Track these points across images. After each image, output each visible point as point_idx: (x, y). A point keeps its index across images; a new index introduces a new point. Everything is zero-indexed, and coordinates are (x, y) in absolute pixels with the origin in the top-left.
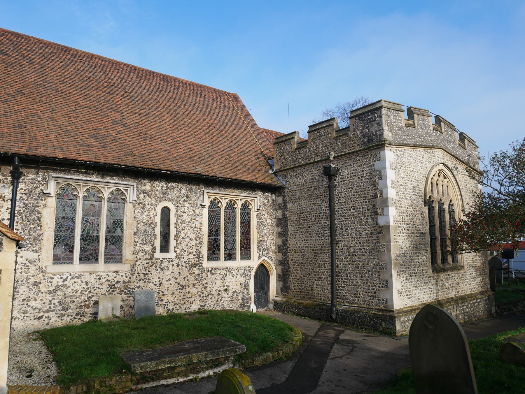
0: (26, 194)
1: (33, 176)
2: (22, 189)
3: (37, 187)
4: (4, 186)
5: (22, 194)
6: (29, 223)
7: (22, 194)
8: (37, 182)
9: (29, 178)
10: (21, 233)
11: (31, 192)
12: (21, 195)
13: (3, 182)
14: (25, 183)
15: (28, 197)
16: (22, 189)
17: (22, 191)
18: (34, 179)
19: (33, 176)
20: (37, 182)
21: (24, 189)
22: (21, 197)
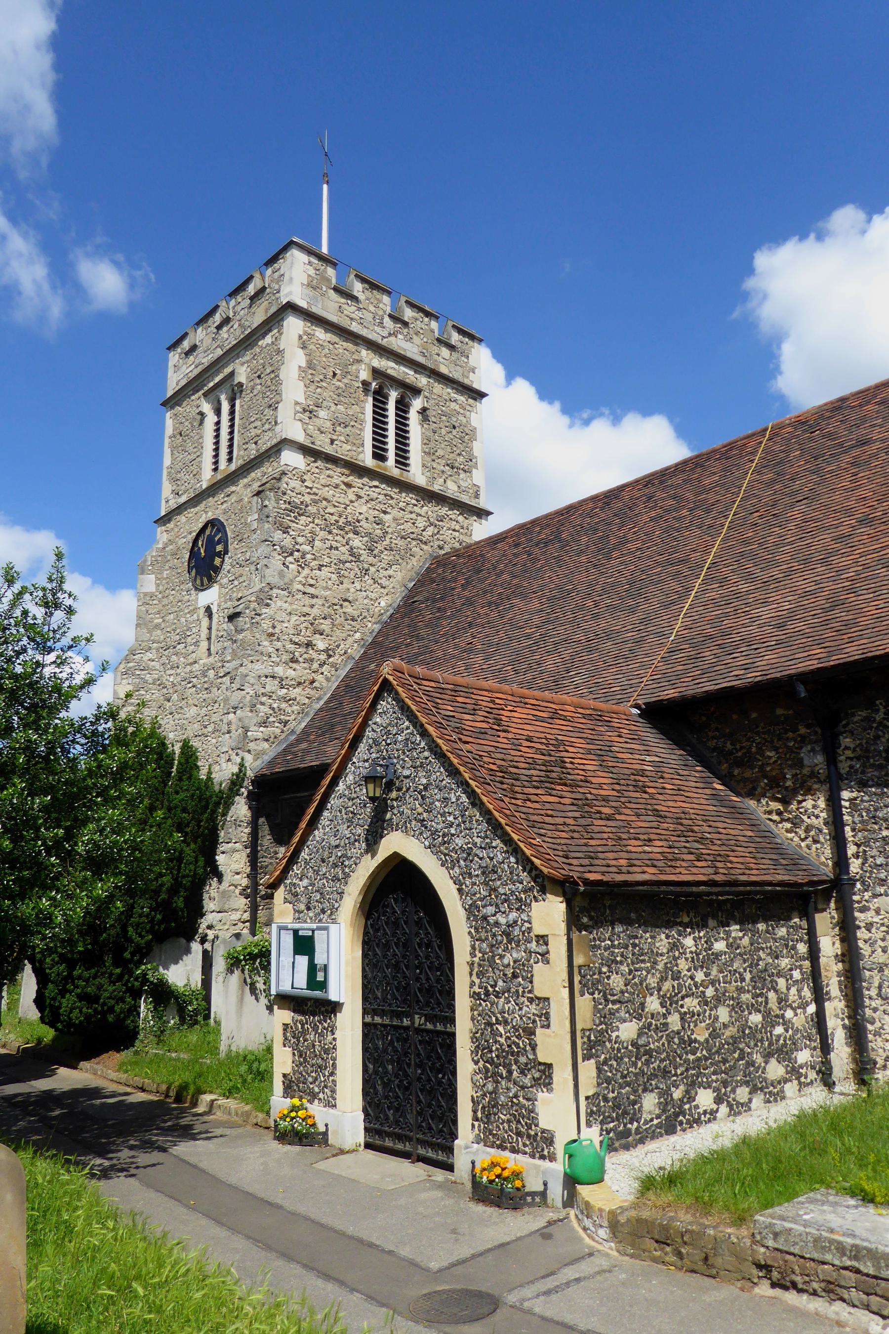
0: (858, 758)
1: (864, 714)
2: (847, 748)
3: (877, 737)
4: (813, 750)
5: (851, 759)
6: (876, 827)
7: (851, 759)
8: (875, 725)
9: (856, 719)
10: (865, 851)
11: (867, 751)
12: (849, 763)
13: (811, 742)
14: (852, 732)
15: (864, 765)
16: (847, 748)
17: (849, 753)
18: (867, 719)
19: (864, 714)
20: (875, 725)
21: (852, 746)
22: (851, 767)
